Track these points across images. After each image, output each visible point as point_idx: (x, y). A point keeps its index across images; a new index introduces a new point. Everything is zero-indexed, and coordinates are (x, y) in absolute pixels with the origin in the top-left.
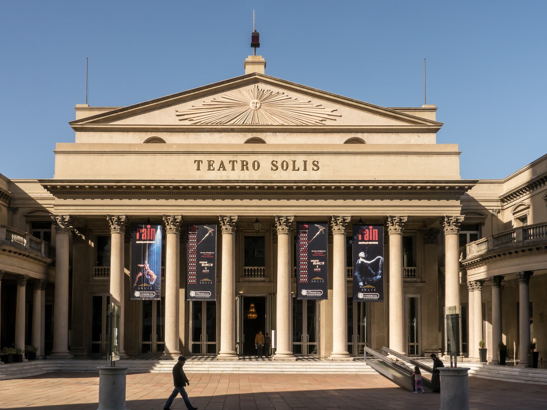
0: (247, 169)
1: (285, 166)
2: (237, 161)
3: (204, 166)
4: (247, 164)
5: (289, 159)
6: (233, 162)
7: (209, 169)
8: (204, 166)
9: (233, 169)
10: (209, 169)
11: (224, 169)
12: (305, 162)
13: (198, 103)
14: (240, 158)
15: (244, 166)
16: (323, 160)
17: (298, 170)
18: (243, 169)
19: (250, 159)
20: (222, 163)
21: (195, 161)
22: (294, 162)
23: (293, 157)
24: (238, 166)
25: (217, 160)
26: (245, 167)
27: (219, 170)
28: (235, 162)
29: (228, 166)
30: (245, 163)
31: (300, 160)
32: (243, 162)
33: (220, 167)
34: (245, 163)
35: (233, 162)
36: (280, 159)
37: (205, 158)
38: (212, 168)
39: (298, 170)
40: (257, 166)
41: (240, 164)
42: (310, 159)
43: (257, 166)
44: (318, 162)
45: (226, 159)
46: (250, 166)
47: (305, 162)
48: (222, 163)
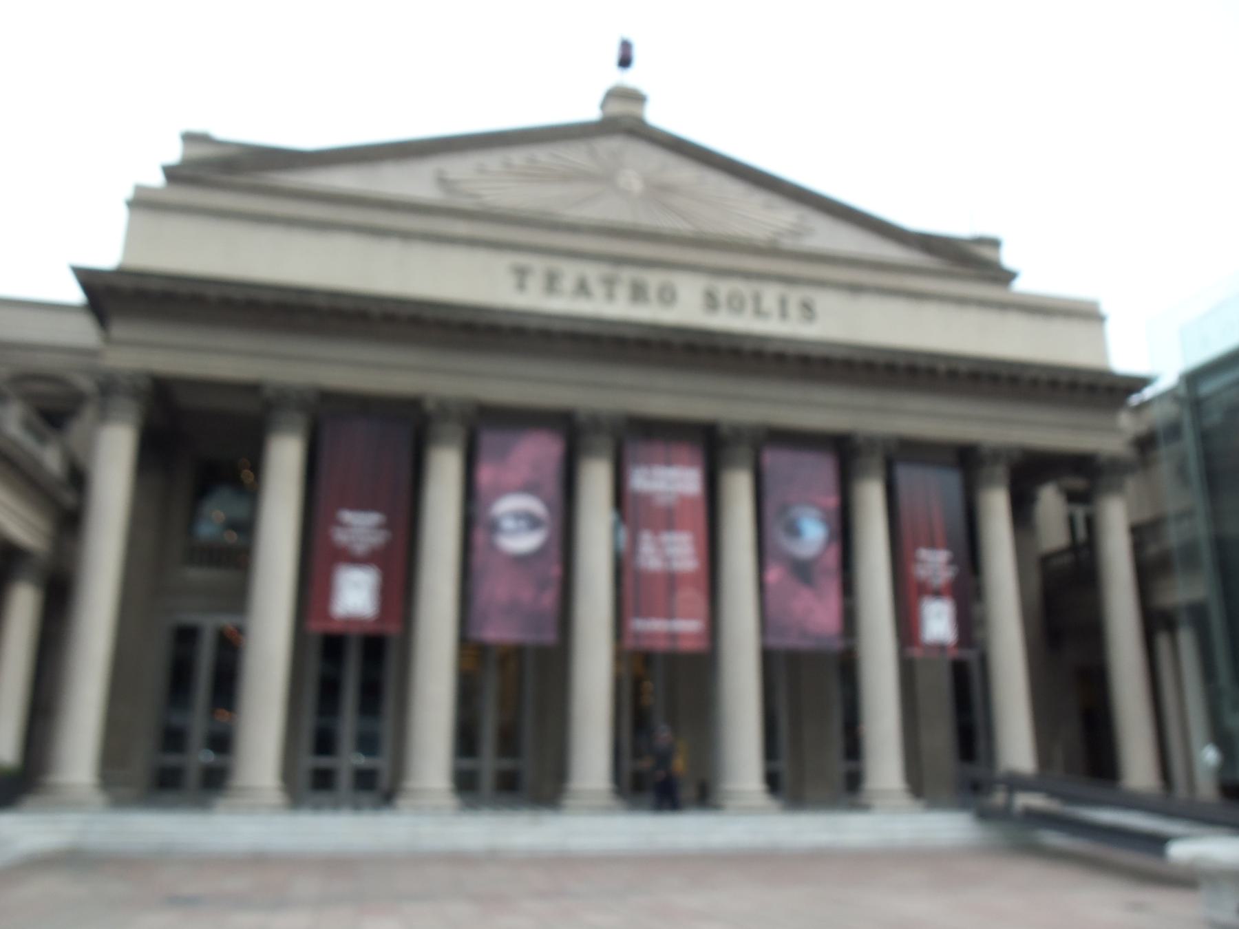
1: (736, 304)
3: (535, 283)
5: (745, 288)
8: (535, 283)
13: (493, 160)
14: (627, 275)
15: (638, 293)
16: (826, 301)
19: (653, 279)
22: (757, 299)
24: (622, 292)
25: (570, 271)
29: (598, 290)
31: (771, 295)
35: (610, 283)
36: (724, 288)
37: (539, 265)
40: (668, 296)
42: (795, 296)
45: (593, 272)
46: (652, 293)
47: (783, 303)
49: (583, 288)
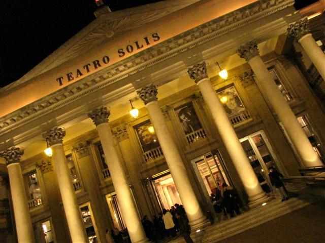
0: (100, 65)
2: (89, 64)
4: (98, 61)
6: (87, 67)
7: (69, 80)
9: (88, 71)
10: (69, 80)
11: (81, 74)
12: (146, 39)
17: (142, 46)
18: (96, 67)
20: (78, 71)
21: (57, 80)
22: (137, 43)
23: (134, 40)
26: (97, 66)
27: (77, 77)
28: (89, 66)
30: (96, 62)
32: (94, 62)
33: (77, 75)
34: (96, 62)
35: (87, 67)
38: (71, 78)
39: (142, 46)
41: (92, 65)
43: (106, 59)
44: (157, 34)
46: (101, 62)
47: (146, 39)
48: (78, 71)
49: (79, 73)
